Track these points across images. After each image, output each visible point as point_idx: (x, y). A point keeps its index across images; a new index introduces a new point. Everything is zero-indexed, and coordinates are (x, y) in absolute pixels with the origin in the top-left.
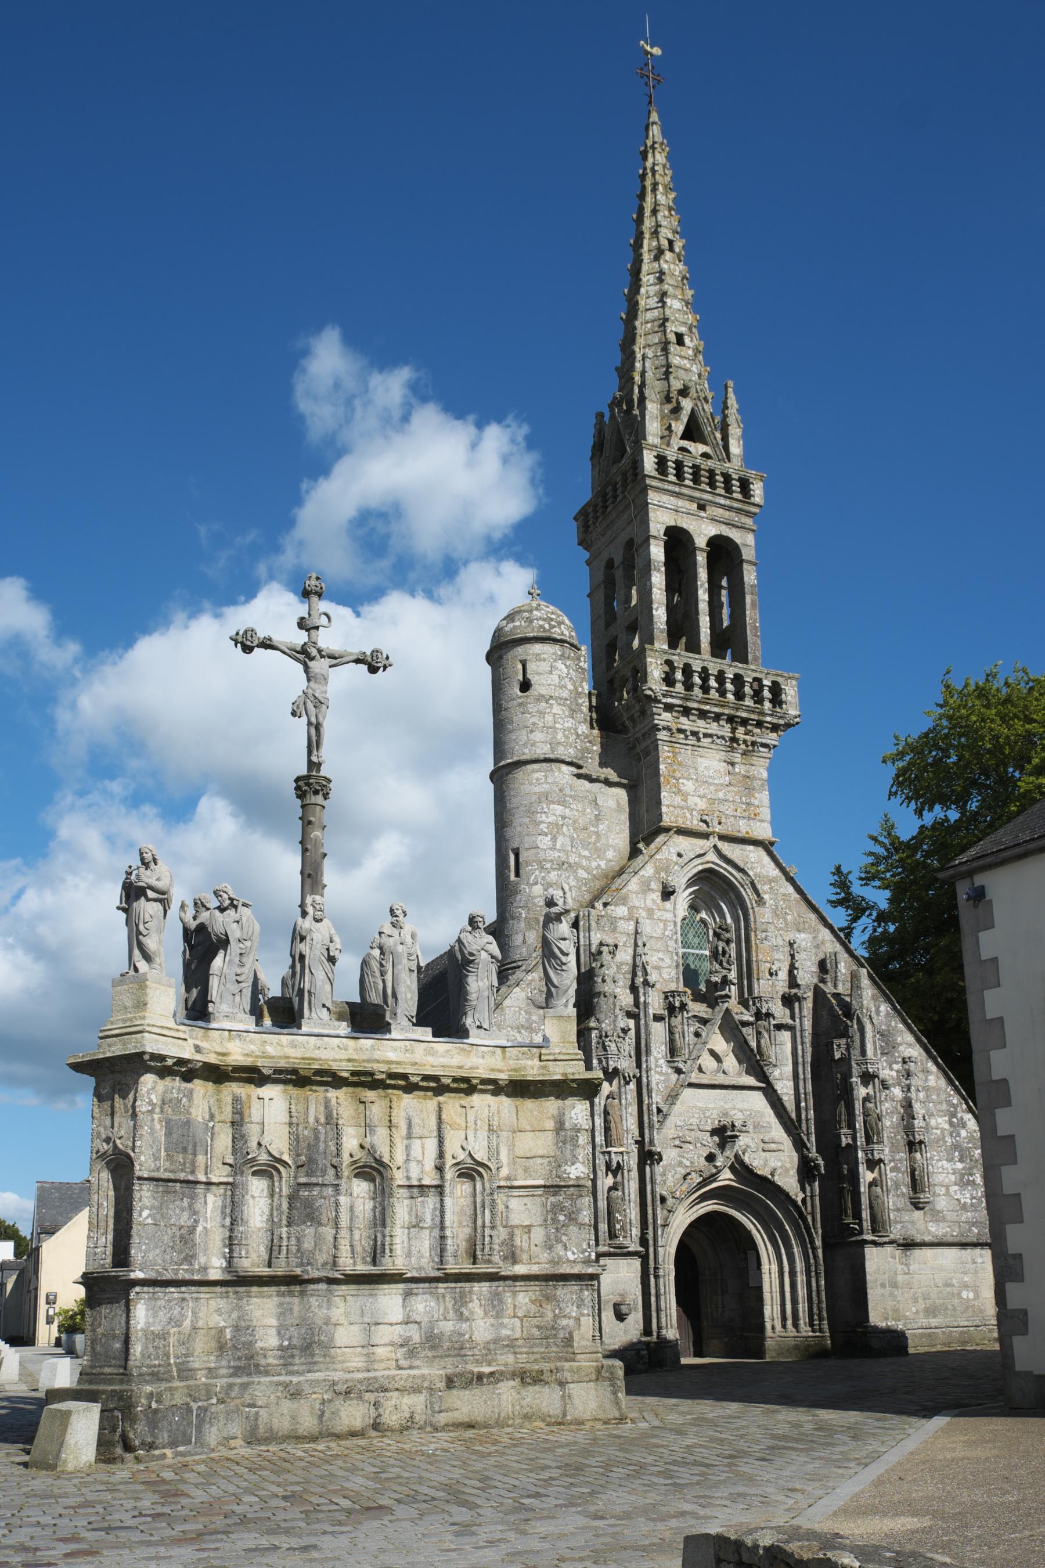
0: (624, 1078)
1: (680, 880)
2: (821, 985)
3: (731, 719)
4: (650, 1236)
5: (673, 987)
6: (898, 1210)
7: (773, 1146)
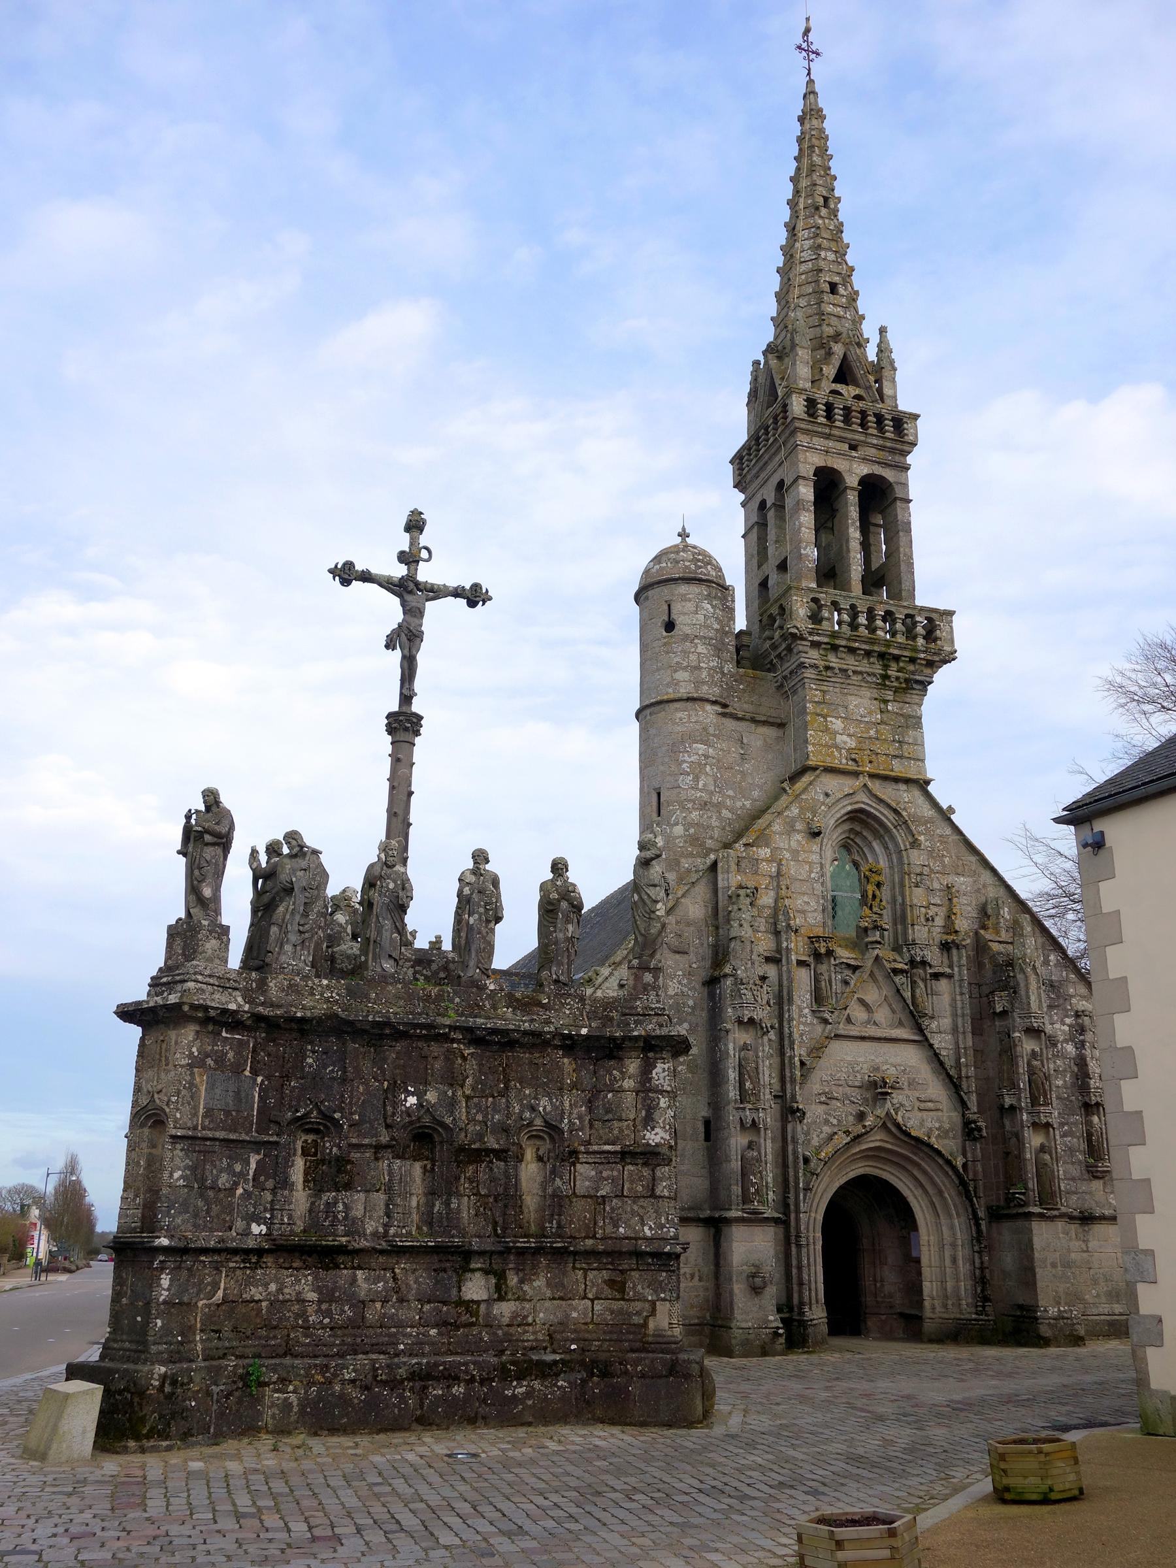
0: (762, 1028)
1: (829, 820)
2: (982, 932)
3: (882, 656)
4: (792, 1201)
5: (819, 931)
6: (1073, 1179)
7: (930, 1105)
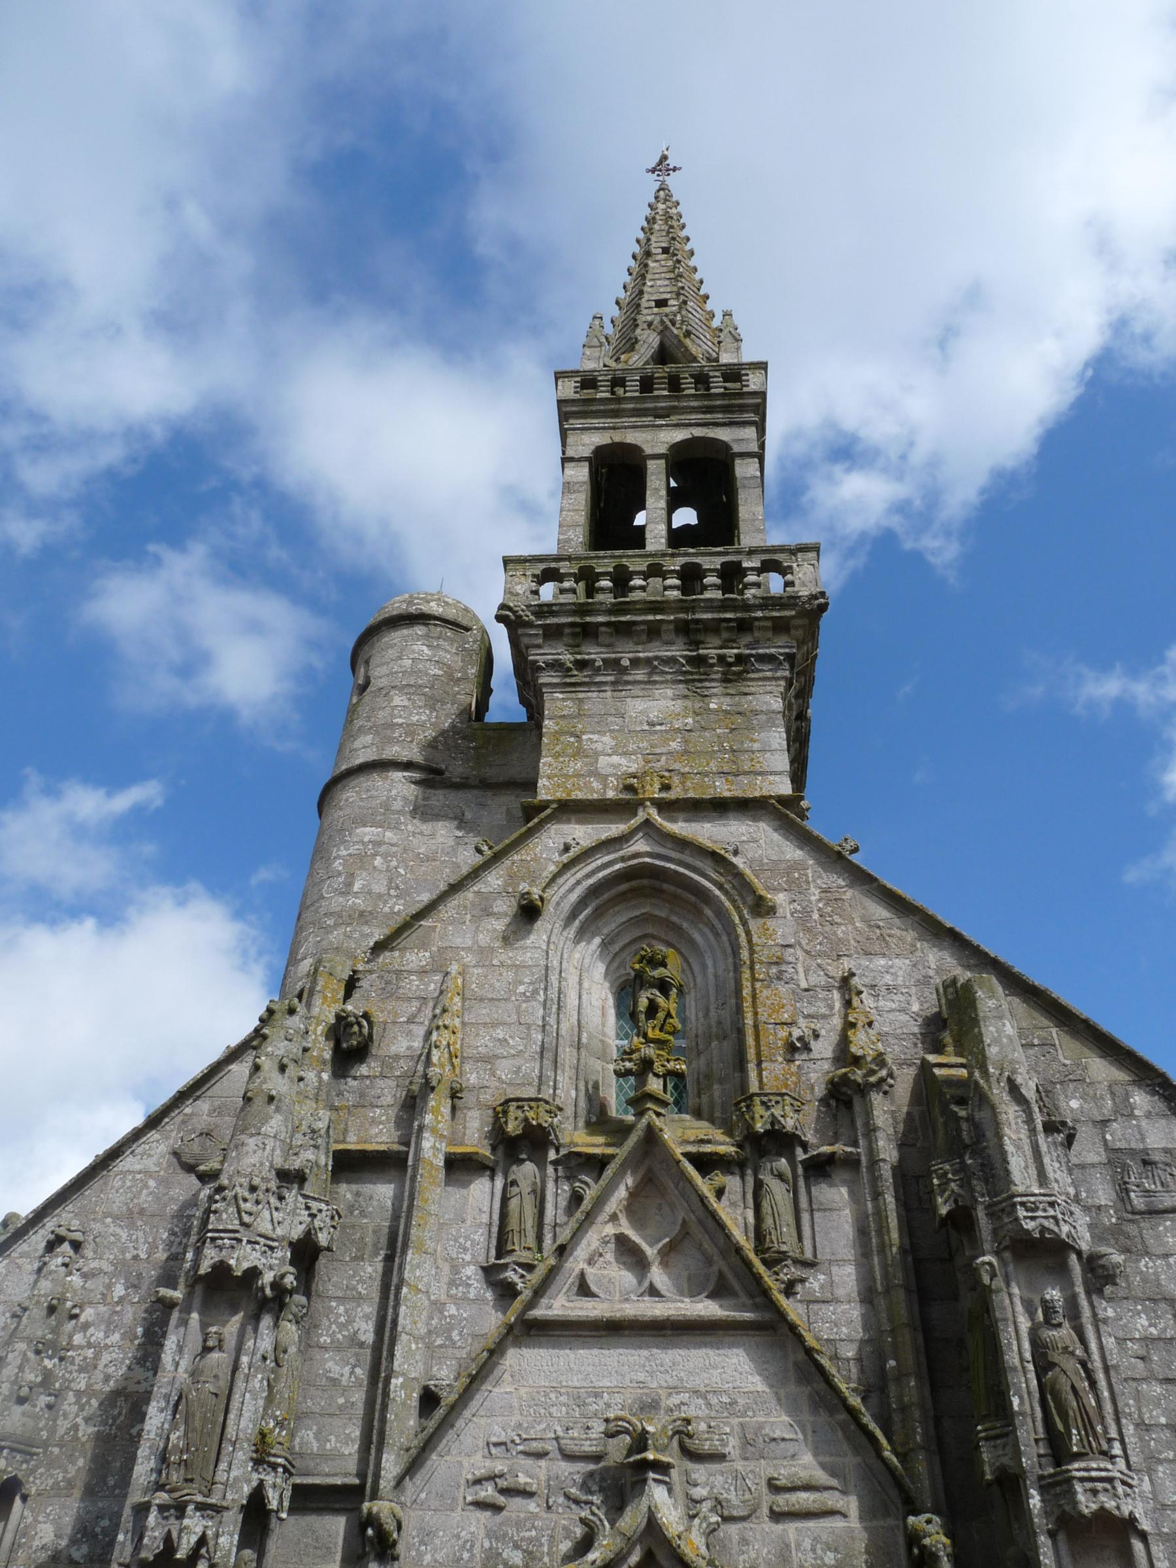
7: (804, 1499)
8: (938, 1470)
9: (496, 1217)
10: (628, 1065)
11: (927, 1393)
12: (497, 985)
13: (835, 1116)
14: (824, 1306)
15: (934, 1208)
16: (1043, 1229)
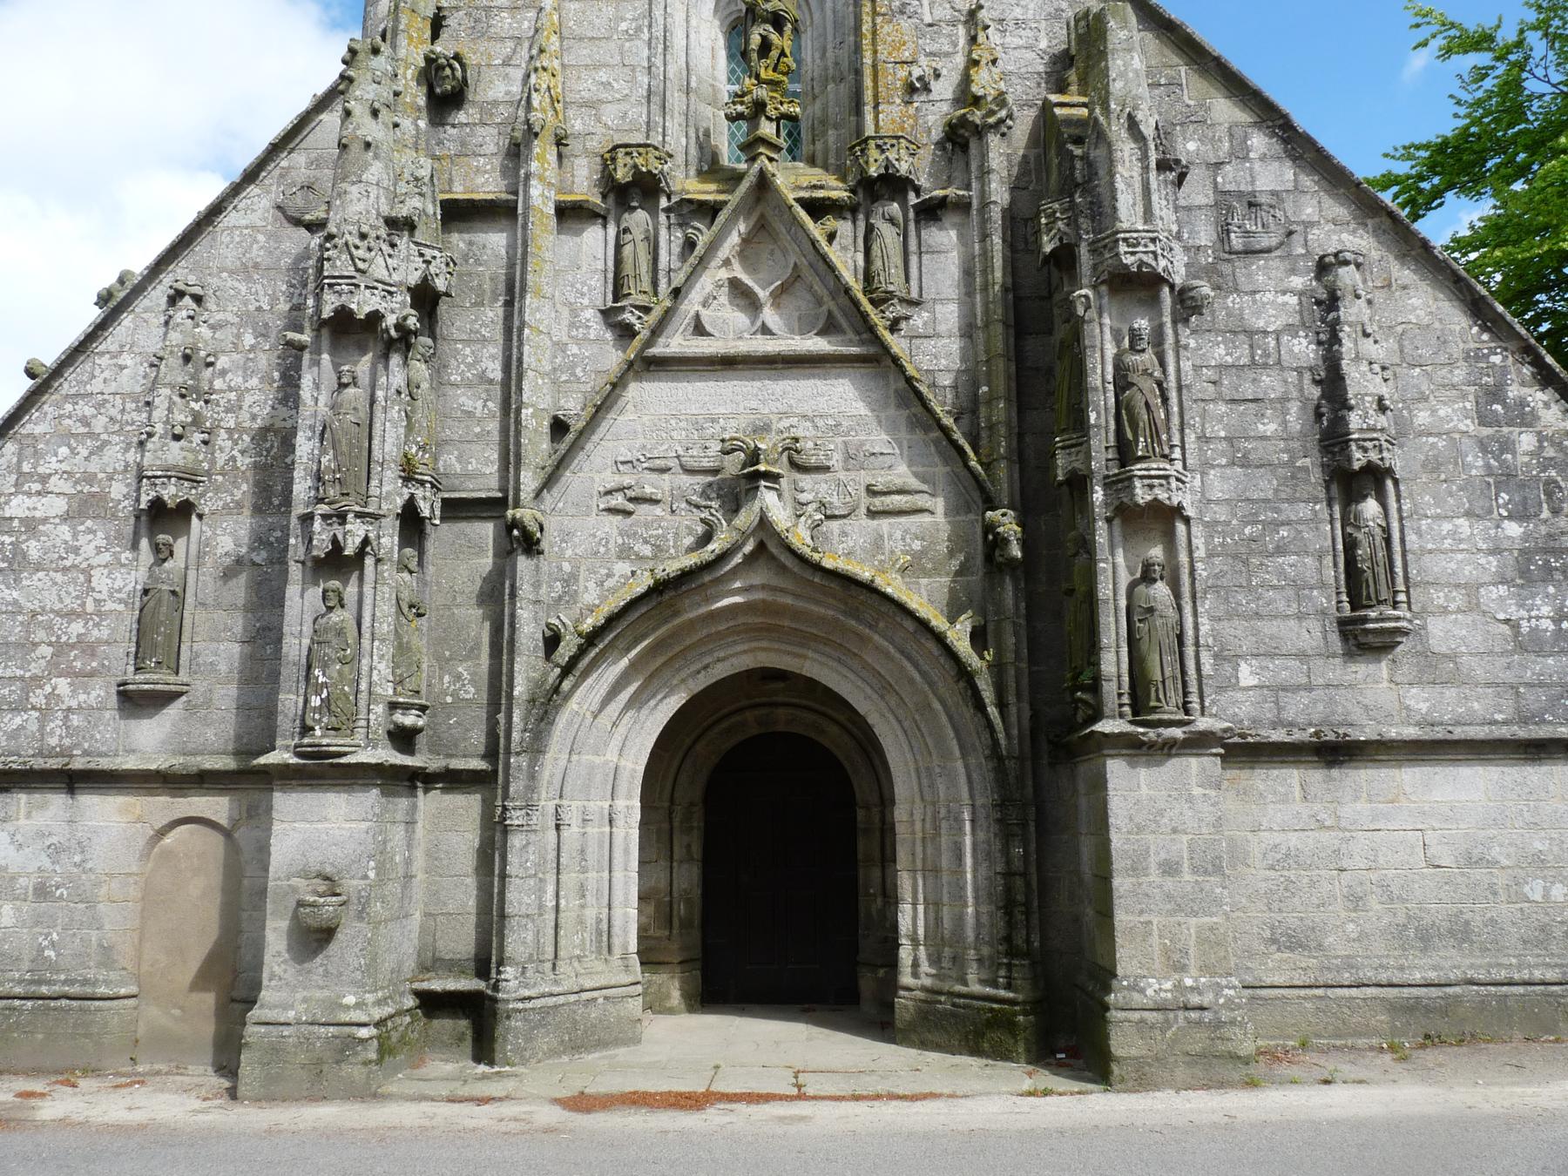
8: (1016, 476)
9: (611, 263)
10: (740, 108)
11: (1014, 414)
12: (597, 21)
13: (950, 160)
14: (925, 341)
15: (1040, 247)
16: (1142, 263)
